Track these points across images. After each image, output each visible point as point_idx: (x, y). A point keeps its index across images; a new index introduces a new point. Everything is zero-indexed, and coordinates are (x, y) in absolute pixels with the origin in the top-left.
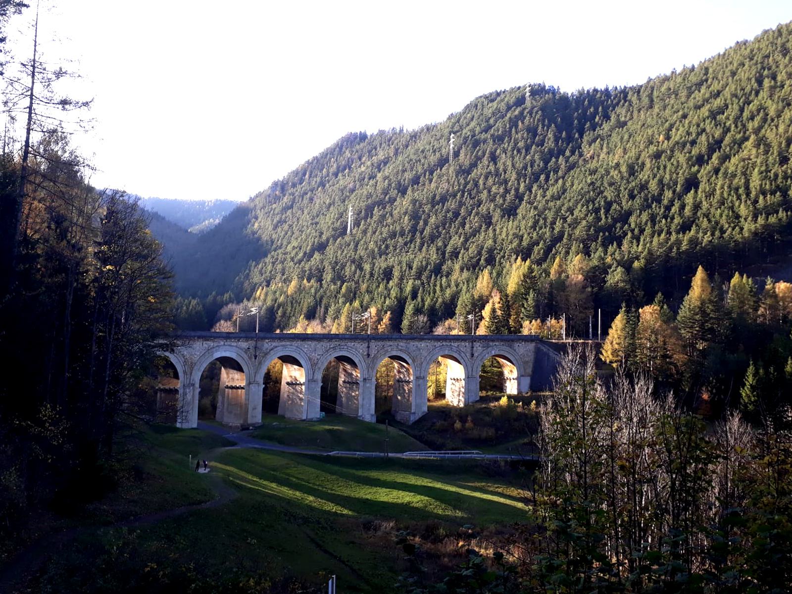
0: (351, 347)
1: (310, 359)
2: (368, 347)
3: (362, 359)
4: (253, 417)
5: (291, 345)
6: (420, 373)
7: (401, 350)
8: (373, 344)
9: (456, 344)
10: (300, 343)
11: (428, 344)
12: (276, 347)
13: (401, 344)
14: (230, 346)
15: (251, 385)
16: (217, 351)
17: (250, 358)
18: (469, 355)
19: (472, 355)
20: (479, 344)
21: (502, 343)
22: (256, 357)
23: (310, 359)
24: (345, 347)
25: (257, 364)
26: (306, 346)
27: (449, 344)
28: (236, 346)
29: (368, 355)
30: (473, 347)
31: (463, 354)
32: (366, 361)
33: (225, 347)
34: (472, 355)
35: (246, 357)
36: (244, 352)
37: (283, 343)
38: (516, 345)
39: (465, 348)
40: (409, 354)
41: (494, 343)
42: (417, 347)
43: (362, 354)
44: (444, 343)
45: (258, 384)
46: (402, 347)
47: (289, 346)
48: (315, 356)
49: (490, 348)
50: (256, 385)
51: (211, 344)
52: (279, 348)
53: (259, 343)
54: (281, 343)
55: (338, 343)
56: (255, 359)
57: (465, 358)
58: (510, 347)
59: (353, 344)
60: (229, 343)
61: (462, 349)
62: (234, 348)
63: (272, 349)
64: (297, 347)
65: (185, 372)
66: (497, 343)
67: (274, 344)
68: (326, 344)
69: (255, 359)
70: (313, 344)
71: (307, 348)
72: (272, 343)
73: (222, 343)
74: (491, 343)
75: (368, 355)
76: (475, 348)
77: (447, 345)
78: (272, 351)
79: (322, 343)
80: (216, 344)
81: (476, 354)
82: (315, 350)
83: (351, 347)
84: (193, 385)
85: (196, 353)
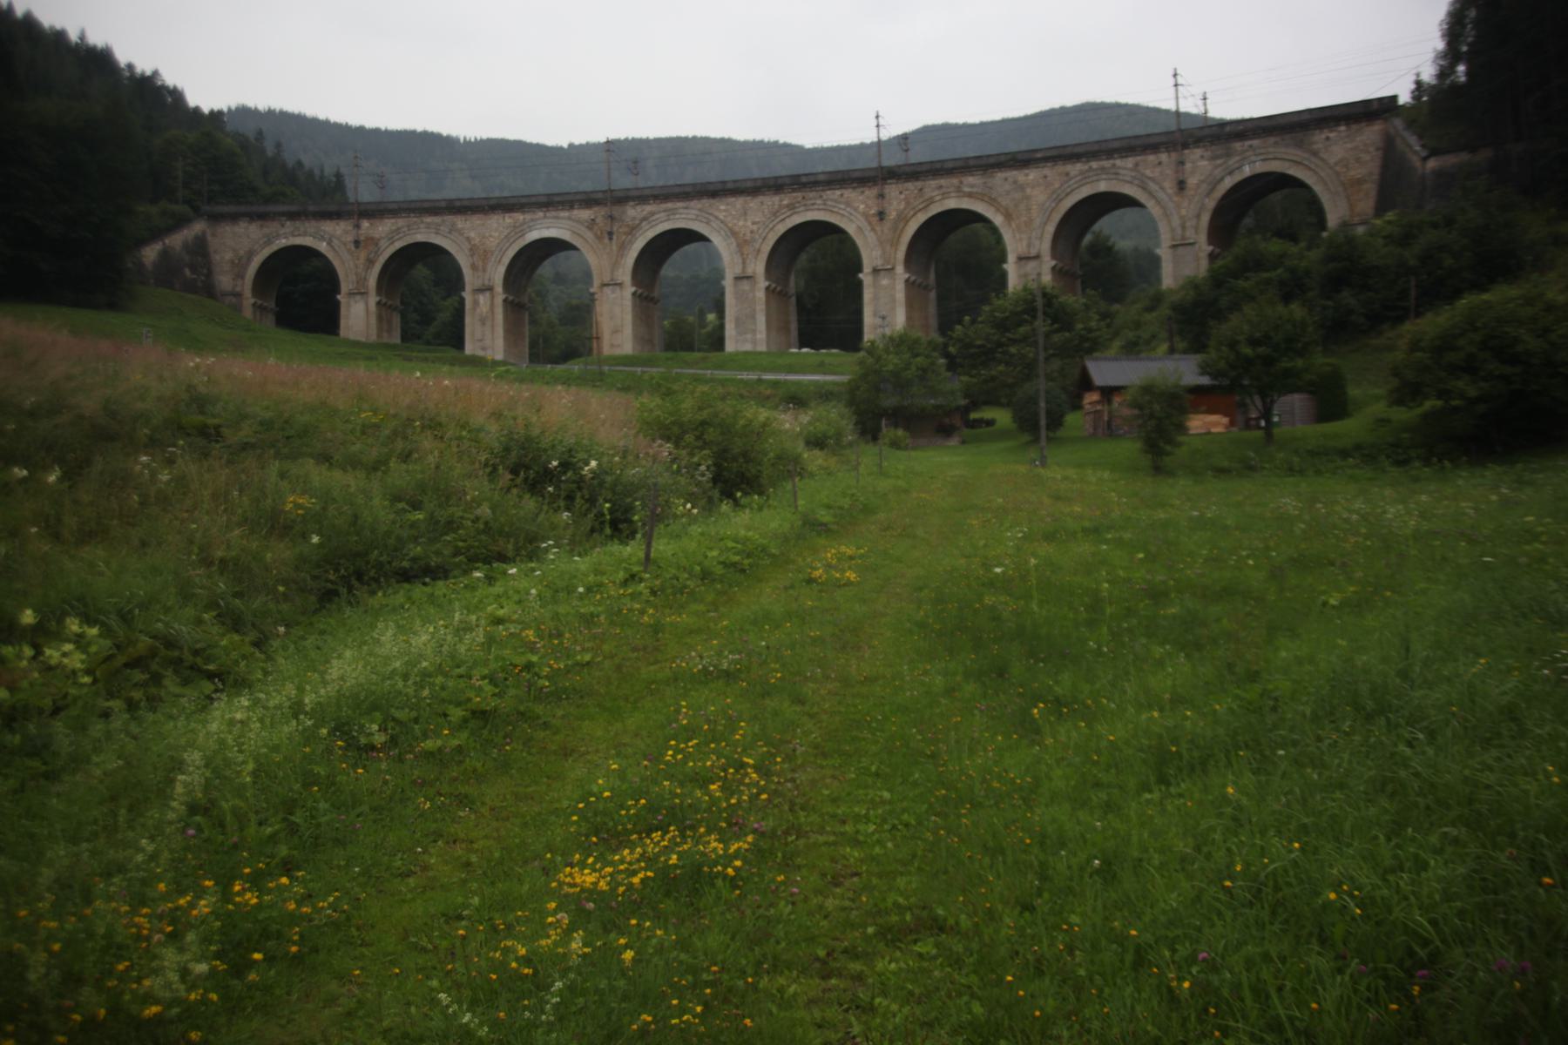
0: (836, 201)
1: (734, 234)
2: (881, 196)
3: (864, 224)
4: (612, 346)
5: (686, 208)
6: (1029, 245)
7: (970, 195)
8: (893, 190)
9: (1129, 162)
10: (706, 202)
11: (1047, 171)
12: (653, 214)
13: (971, 179)
14: (557, 218)
15: (605, 288)
16: (531, 229)
17: (599, 238)
18: (1169, 185)
19: (1181, 185)
20: (1198, 152)
21: (1272, 140)
22: (610, 234)
23: (734, 234)
24: (819, 202)
25: (614, 248)
26: (723, 207)
27: (1107, 164)
28: (569, 218)
29: (881, 215)
30: (1182, 163)
31: (1152, 186)
32: (878, 228)
33: (546, 220)
34: (1181, 185)
35: (589, 235)
36: (588, 227)
37: (669, 205)
38: (1318, 137)
39: (1158, 170)
40: (992, 202)
41: (1249, 143)
42: (1015, 182)
43: (866, 215)
44: (1094, 165)
45: (620, 285)
46: (972, 186)
47: (681, 211)
48: (745, 226)
49: (1233, 161)
50: (618, 288)
51: (520, 217)
52: (657, 216)
53: (616, 211)
54: (664, 206)
55: (799, 195)
56: (611, 239)
57: (1161, 195)
58: (1299, 145)
59: (838, 192)
60: (554, 213)
61: (1148, 172)
62: (564, 221)
63: (645, 219)
64: (700, 210)
65: (474, 267)
66: (1255, 142)
67: (648, 208)
68: (771, 201)
69: (611, 239)
70: (739, 202)
71: (725, 211)
72: (644, 207)
73: (541, 214)
74: (1238, 145)
75: (881, 215)
76: (1188, 166)
77: (1103, 169)
78: (644, 223)
79: (761, 198)
80: (528, 217)
81: (1192, 181)
82: (745, 214)
83: (836, 201)
84: (490, 289)
85: (493, 234)
